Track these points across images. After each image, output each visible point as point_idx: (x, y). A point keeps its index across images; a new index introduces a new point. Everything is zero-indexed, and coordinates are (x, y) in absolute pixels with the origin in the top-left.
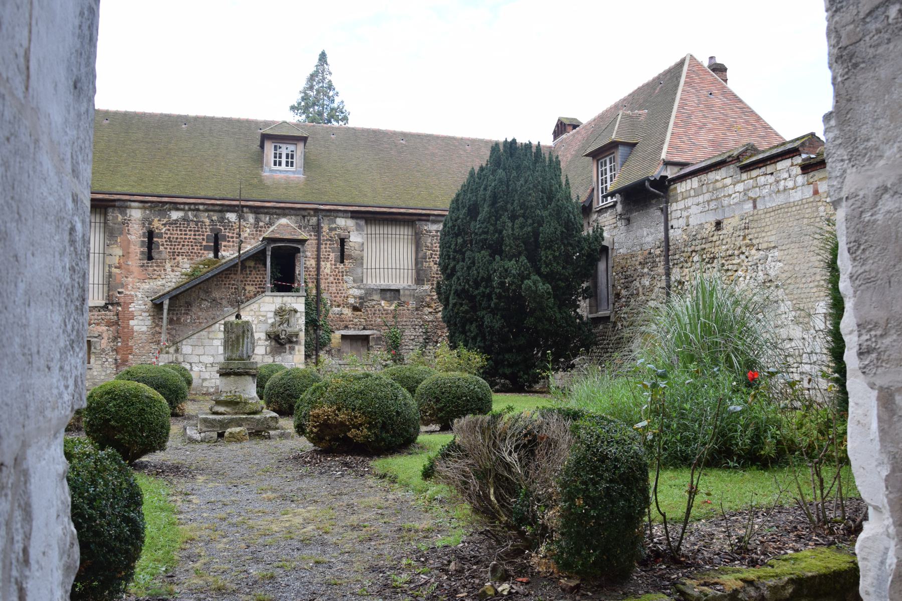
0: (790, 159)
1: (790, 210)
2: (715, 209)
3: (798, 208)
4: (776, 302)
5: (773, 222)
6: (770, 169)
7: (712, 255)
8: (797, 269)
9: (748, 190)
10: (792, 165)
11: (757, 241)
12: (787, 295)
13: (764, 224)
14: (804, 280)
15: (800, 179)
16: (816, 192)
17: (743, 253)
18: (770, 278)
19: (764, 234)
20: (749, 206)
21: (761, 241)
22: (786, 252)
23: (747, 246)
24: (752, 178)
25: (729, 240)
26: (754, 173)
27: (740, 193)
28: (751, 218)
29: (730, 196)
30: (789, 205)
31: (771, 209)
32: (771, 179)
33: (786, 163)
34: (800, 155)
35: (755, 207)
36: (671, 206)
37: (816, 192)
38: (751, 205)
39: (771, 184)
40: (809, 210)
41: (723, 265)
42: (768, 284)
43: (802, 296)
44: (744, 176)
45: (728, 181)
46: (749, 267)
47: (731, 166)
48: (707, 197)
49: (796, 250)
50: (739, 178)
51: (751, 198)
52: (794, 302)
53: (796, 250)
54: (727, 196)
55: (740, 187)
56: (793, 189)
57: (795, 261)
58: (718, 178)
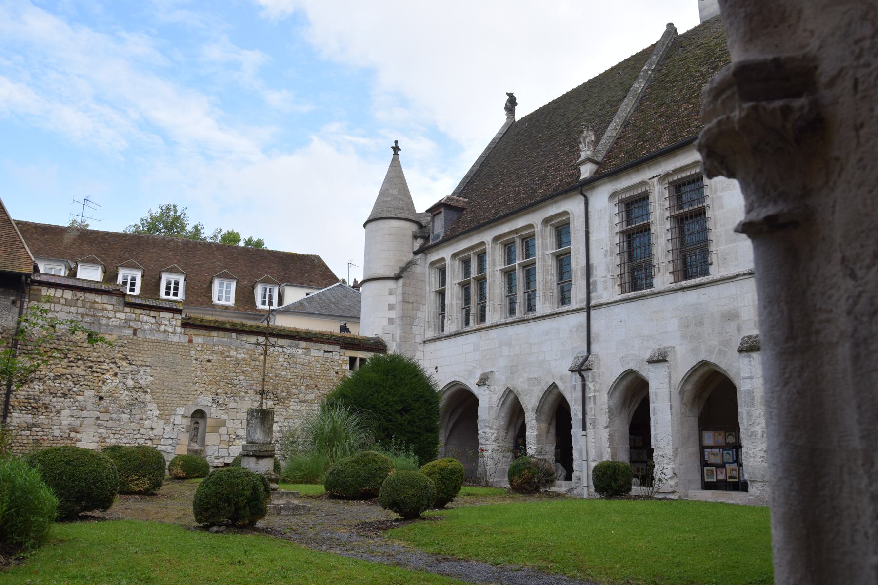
0: (172, 314)
1: (167, 345)
2: (91, 323)
3: (174, 346)
4: (143, 402)
5: (150, 349)
6: (153, 313)
7: (79, 357)
8: (166, 384)
9: (130, 321)
10: (173, 318)
11: (133, 358)
12: (154, 399)
13: (142, 349)
14: (170, 392)
15: (179, 330)
16: (190, 341)
17: (115, 363)
18: (140, 386)
19: (139, 355)
20: (130, 332)
21: (136, 359)
22: (158, 371)
23: (120, 358)
24: (135, 314)
25: (102, 350)
26: (138, 311)
27: (121, 320)
28: (130, 341)
29: (109, 318)
30: (166, 342)
31: (150, 340)
32: (153, 320)
33: (170, 315)
34: (181, 315)
35: (135, 334)
36: (29, 302)
37: (190, 341)
38: (131, 332)
39: (152, 324)
40: (183, 351)
41: (91, 367)
42: (137, 390)
43: (167, 402)
44: (127, 309)
45: (110, 307)
46: (119, 375)
47: (115, 298)
48: (81, 310)
49: (168, 372)
50: (122, 309)
51: (132, 327)
52: (160, 405)
53: (168, 372)
54: (106, 318)
55: (122, 316)
56: (172, 333)
57: (165, 379)
58: (97, 300)
